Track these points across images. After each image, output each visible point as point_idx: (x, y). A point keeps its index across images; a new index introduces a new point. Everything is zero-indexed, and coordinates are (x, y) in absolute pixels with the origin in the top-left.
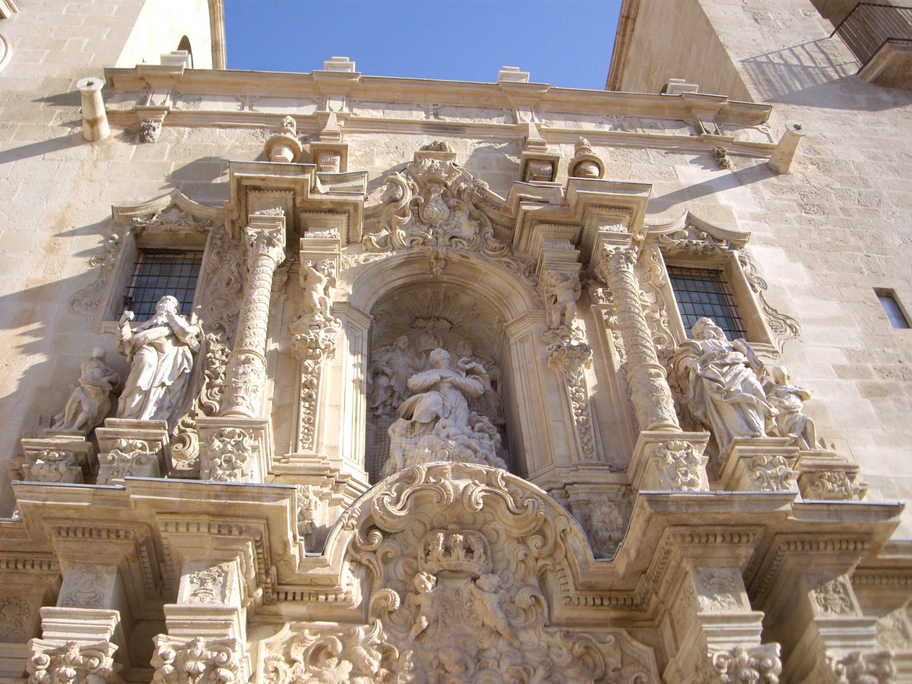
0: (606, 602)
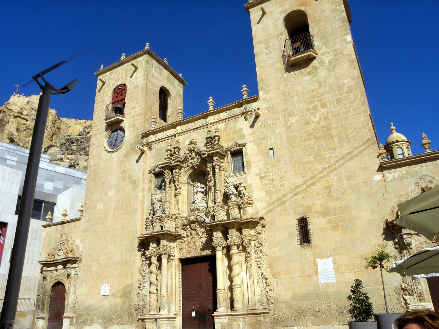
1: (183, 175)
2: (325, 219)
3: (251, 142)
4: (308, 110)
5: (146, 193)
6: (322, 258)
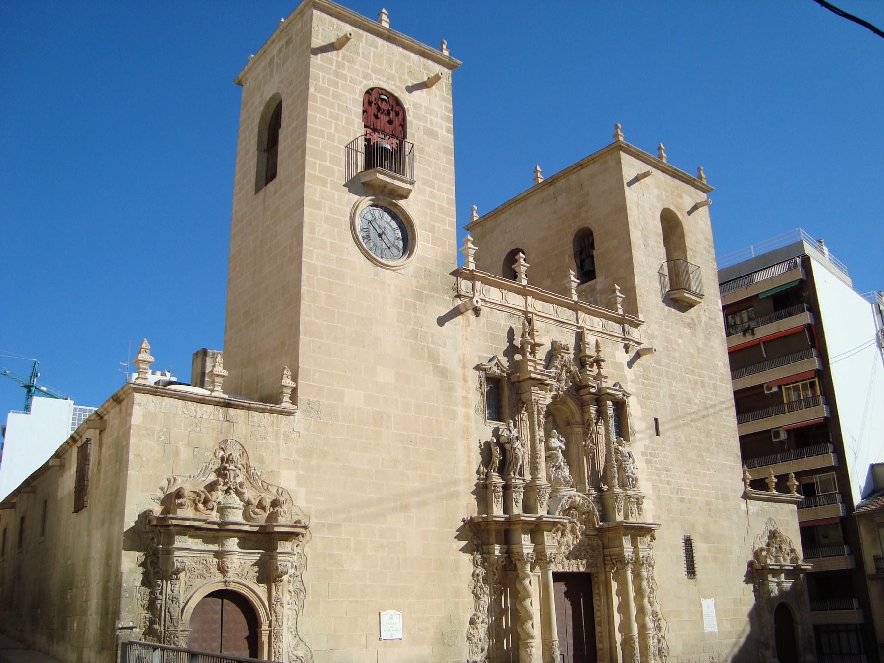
2: (706, 545)
4: (690, 381)
5: (472, 412)
6: (706, 598)
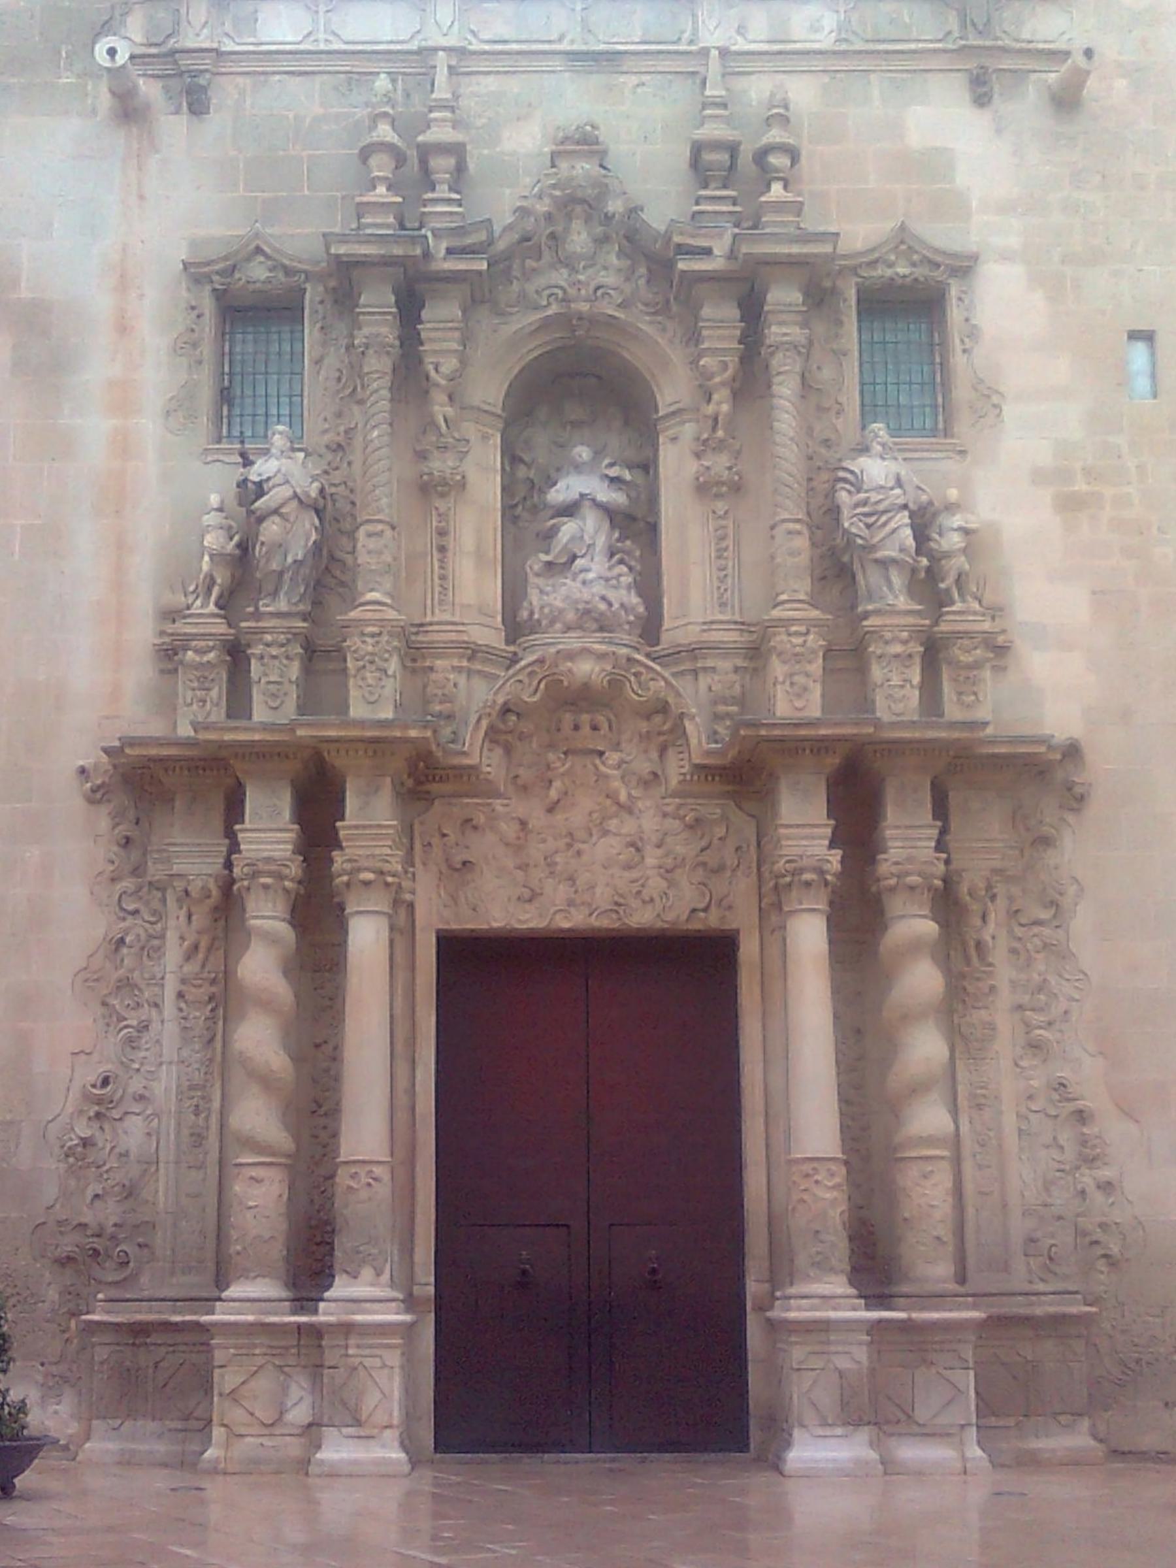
0: (717, 778)
1: (478, 363)
3: (1006, 257)
5: (149, 426)
